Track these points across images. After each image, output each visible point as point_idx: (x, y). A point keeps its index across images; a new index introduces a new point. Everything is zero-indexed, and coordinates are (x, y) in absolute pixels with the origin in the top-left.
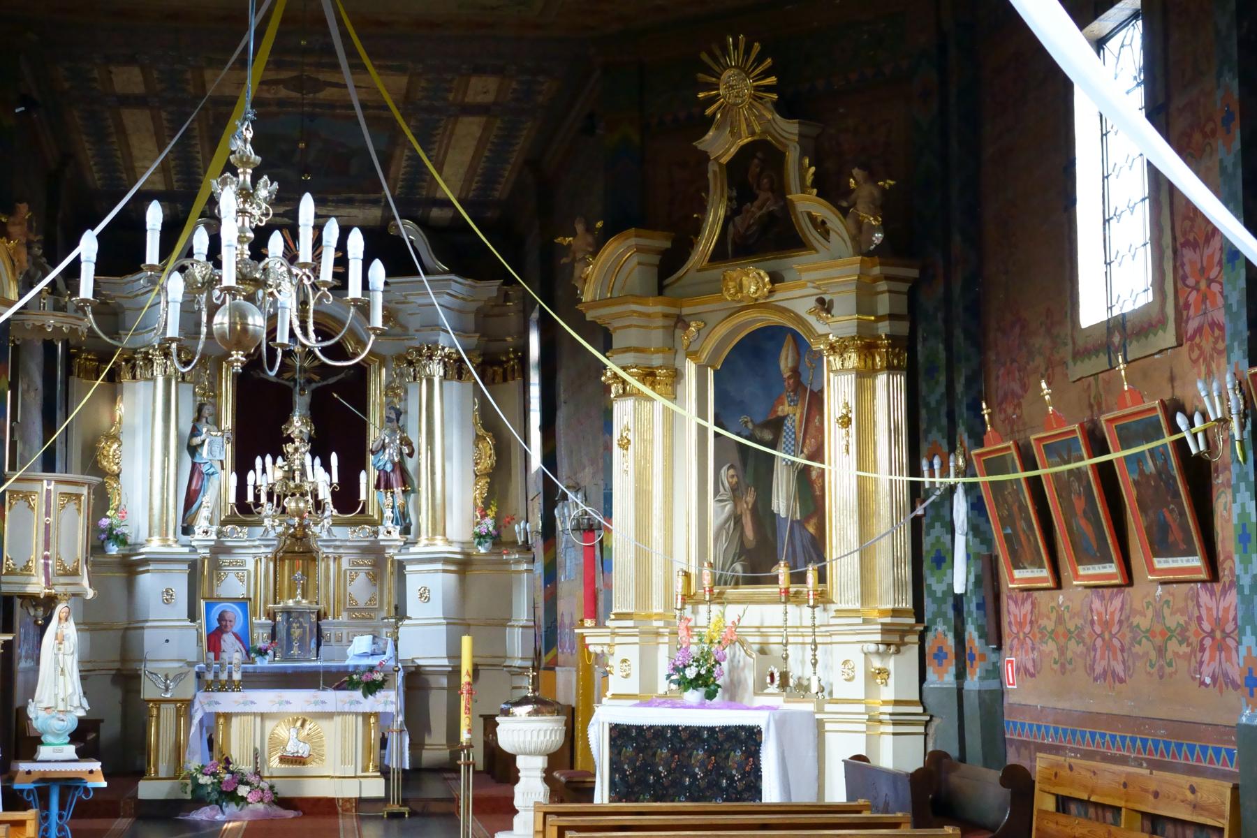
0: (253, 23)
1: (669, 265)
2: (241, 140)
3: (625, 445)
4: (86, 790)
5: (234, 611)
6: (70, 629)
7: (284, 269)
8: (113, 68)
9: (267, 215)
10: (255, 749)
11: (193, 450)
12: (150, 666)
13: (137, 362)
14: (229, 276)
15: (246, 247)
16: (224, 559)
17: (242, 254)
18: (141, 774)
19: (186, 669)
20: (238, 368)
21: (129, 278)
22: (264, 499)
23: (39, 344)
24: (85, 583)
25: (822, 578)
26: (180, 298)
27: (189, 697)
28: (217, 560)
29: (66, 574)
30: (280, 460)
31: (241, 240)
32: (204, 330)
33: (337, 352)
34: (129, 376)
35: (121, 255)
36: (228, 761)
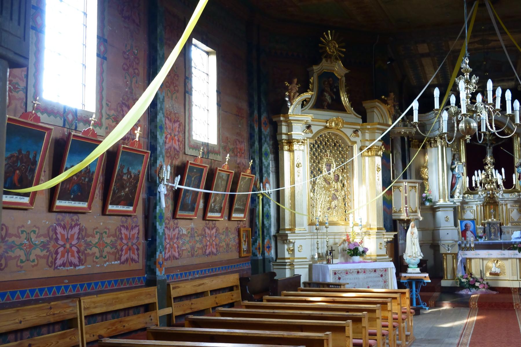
0: (466, 22)
2: (465, 64)
4: (424, 283)
5: (470, 223)
6: (416, 230)
7: (483, 106)
9: (475, 88)
10: (481, 270)
11: (453, 170)
12: (443, 242)
13: (432, 142)
14: (464, 110)
15: (469, 100)
16: (466, 206)
17: (467, 102)
18: (442, 278)
19: (455, 243)
20: (468, 141)
21: (427, 114)
22: (478, 185)
23: (399, 138)
24: (419, 215)
26: (447, 119)
27: (457, 252)
28: (463, 206)
29: (413, 212)
30: (483, 172)
31: (467, 98)
32: (456, 129)
33: (502, 133)
34: (429, 146)
35: (427, 106)
36: (471, 274)
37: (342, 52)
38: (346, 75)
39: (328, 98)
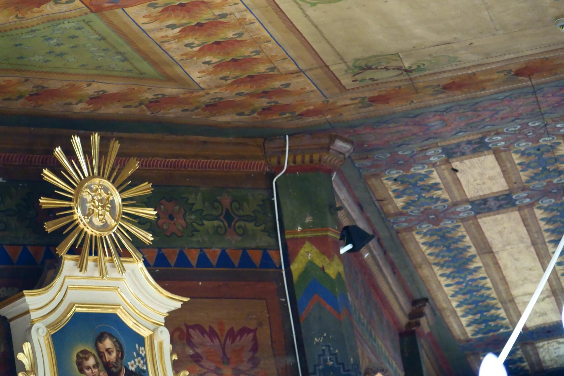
8: (456, 164)
37: (141, 222)
38: (171, 320)
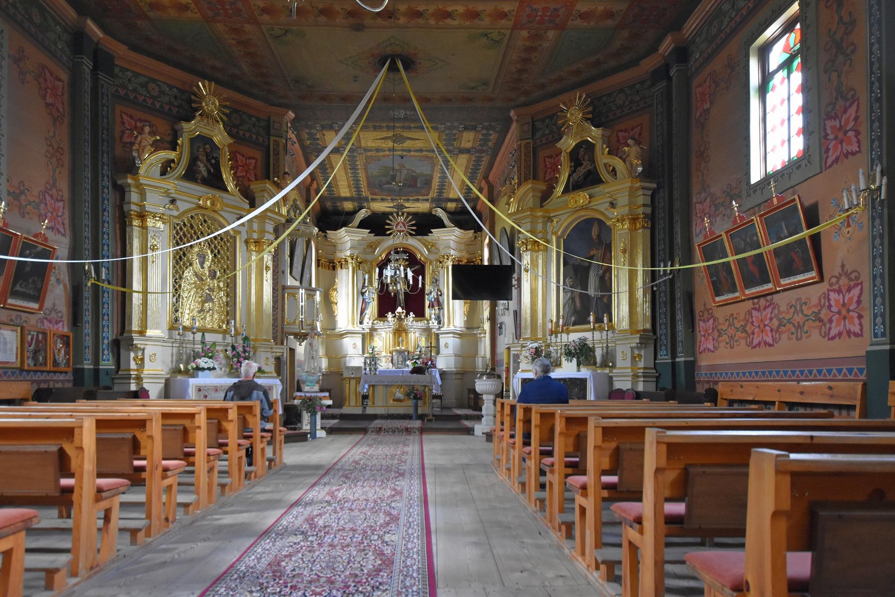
1: (546, 196)
3: (527, 271)
25: (610, 320)
39: (202, 168)
